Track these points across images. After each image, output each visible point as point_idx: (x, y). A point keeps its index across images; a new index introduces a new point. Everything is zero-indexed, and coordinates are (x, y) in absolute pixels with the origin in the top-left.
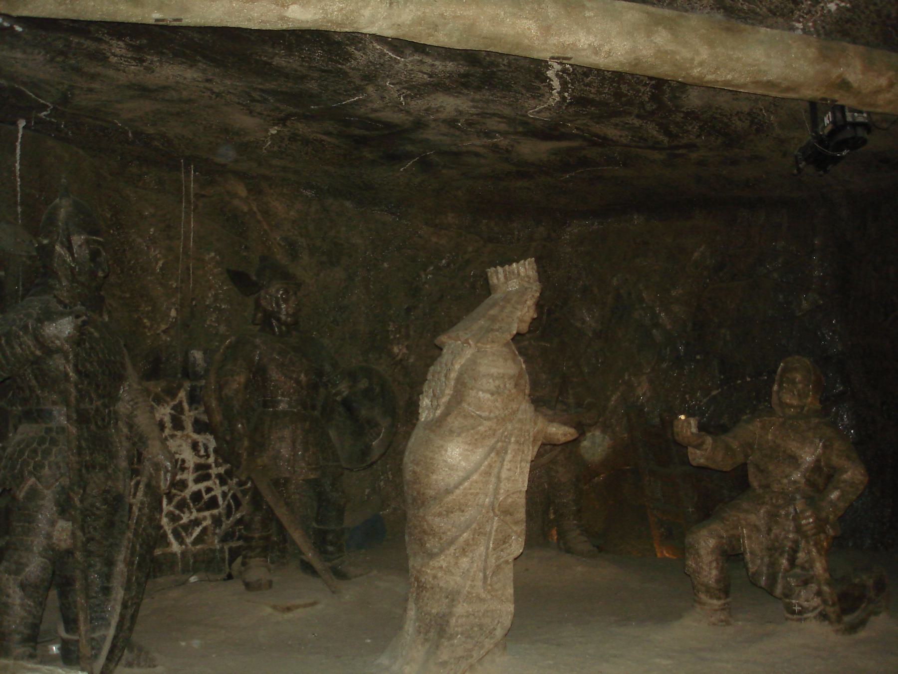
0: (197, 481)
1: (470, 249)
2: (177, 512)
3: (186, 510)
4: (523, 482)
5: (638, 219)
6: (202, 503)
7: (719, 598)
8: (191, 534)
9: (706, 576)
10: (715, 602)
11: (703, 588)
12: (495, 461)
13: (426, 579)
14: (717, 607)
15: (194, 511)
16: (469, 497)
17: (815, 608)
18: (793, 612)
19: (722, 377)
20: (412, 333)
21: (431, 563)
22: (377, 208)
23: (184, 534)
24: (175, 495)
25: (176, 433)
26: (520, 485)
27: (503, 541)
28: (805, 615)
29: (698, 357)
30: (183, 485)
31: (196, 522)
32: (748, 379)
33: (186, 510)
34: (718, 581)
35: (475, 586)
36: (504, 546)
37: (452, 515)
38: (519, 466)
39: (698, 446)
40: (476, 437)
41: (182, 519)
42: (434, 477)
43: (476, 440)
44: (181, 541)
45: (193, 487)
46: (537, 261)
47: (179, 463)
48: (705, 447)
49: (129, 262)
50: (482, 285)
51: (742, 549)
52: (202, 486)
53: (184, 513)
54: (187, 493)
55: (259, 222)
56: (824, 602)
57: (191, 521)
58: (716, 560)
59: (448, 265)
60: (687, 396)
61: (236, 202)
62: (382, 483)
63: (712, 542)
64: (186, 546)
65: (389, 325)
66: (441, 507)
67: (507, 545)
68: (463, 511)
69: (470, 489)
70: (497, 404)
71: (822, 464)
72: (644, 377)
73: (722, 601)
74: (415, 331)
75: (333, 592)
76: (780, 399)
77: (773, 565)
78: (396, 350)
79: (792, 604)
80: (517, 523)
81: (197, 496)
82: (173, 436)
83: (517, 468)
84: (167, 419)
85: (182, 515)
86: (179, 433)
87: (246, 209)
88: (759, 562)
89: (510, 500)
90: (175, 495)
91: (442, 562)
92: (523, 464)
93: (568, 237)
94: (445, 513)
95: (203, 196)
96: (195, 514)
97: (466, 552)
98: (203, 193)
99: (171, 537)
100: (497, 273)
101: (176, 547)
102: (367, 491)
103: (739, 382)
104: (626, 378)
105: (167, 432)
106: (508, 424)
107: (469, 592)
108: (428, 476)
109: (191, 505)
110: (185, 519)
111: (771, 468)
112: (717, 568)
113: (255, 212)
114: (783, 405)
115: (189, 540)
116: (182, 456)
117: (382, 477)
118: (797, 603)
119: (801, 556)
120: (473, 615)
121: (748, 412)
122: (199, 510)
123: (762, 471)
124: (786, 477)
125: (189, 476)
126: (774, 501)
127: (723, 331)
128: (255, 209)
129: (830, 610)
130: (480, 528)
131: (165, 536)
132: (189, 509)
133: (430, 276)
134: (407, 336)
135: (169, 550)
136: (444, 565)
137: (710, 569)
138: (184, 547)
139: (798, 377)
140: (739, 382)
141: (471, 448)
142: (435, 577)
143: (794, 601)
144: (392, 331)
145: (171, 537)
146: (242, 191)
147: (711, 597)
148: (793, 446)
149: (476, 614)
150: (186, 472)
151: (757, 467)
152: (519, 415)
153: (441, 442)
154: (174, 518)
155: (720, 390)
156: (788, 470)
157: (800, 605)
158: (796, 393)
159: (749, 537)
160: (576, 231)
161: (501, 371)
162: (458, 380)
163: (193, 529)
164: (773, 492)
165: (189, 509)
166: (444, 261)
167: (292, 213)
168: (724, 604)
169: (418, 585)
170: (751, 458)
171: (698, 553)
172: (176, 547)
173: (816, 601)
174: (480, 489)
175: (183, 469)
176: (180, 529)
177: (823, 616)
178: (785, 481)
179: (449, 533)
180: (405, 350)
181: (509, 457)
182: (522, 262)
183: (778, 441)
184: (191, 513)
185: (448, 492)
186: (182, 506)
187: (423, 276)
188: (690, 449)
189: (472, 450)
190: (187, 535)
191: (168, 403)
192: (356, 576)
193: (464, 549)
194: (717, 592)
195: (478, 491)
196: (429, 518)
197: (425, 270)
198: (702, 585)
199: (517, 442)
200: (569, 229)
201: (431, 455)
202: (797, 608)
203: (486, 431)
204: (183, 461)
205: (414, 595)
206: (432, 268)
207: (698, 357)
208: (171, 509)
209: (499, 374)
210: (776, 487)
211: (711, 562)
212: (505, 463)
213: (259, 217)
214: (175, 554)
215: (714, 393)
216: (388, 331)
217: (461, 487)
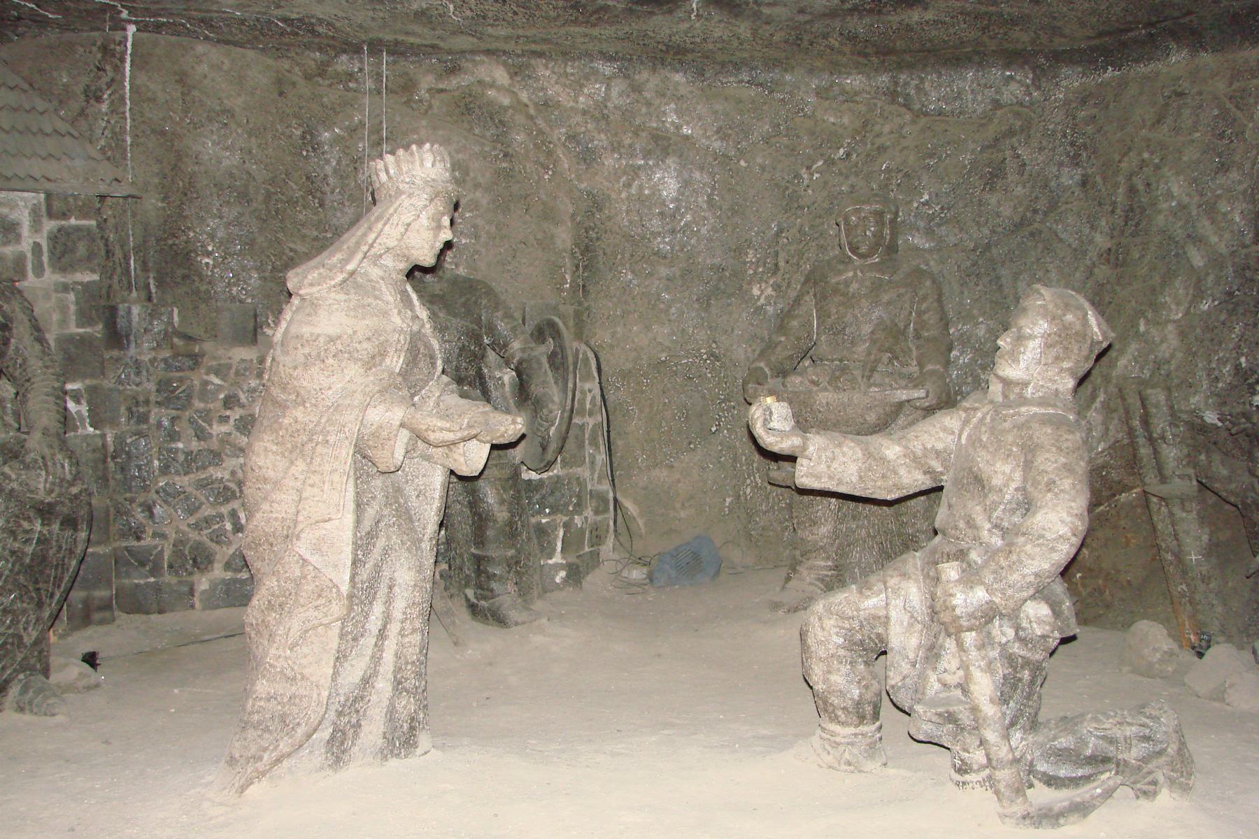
1: (887, 129)
14: (838, 739)
20: (782, 264)
22: (732, 79)
36: (319, 602)
50: (899, 185)
55: (531, 118)
59: (848, 155)
62: (749, 490)
65: (747, 254)
72: (1170, 327)
73: (851, 730)
75: (456, 644)
87: (506, 101)
93: (1061, 96)
95: (442, 91)
98: (441, 86)
102: (728, 500)
104: (1142, 328)
113: (526, 106)
117: (748, 481)
120: (276, 699)
133: (816, 176)
144: (752, 263)
149: (279, 698)
160: (1076, 84)
166: (842, 151)
167: (581, 99)
168: (856, 735)
180: (769, 291)
187: (805, 176)
192: (517, 624)
200: (1064, 83)
202: (958, 762)
206: (820, 163)
209: (312, 334)
213: (532, 111)
216: (745, 263)
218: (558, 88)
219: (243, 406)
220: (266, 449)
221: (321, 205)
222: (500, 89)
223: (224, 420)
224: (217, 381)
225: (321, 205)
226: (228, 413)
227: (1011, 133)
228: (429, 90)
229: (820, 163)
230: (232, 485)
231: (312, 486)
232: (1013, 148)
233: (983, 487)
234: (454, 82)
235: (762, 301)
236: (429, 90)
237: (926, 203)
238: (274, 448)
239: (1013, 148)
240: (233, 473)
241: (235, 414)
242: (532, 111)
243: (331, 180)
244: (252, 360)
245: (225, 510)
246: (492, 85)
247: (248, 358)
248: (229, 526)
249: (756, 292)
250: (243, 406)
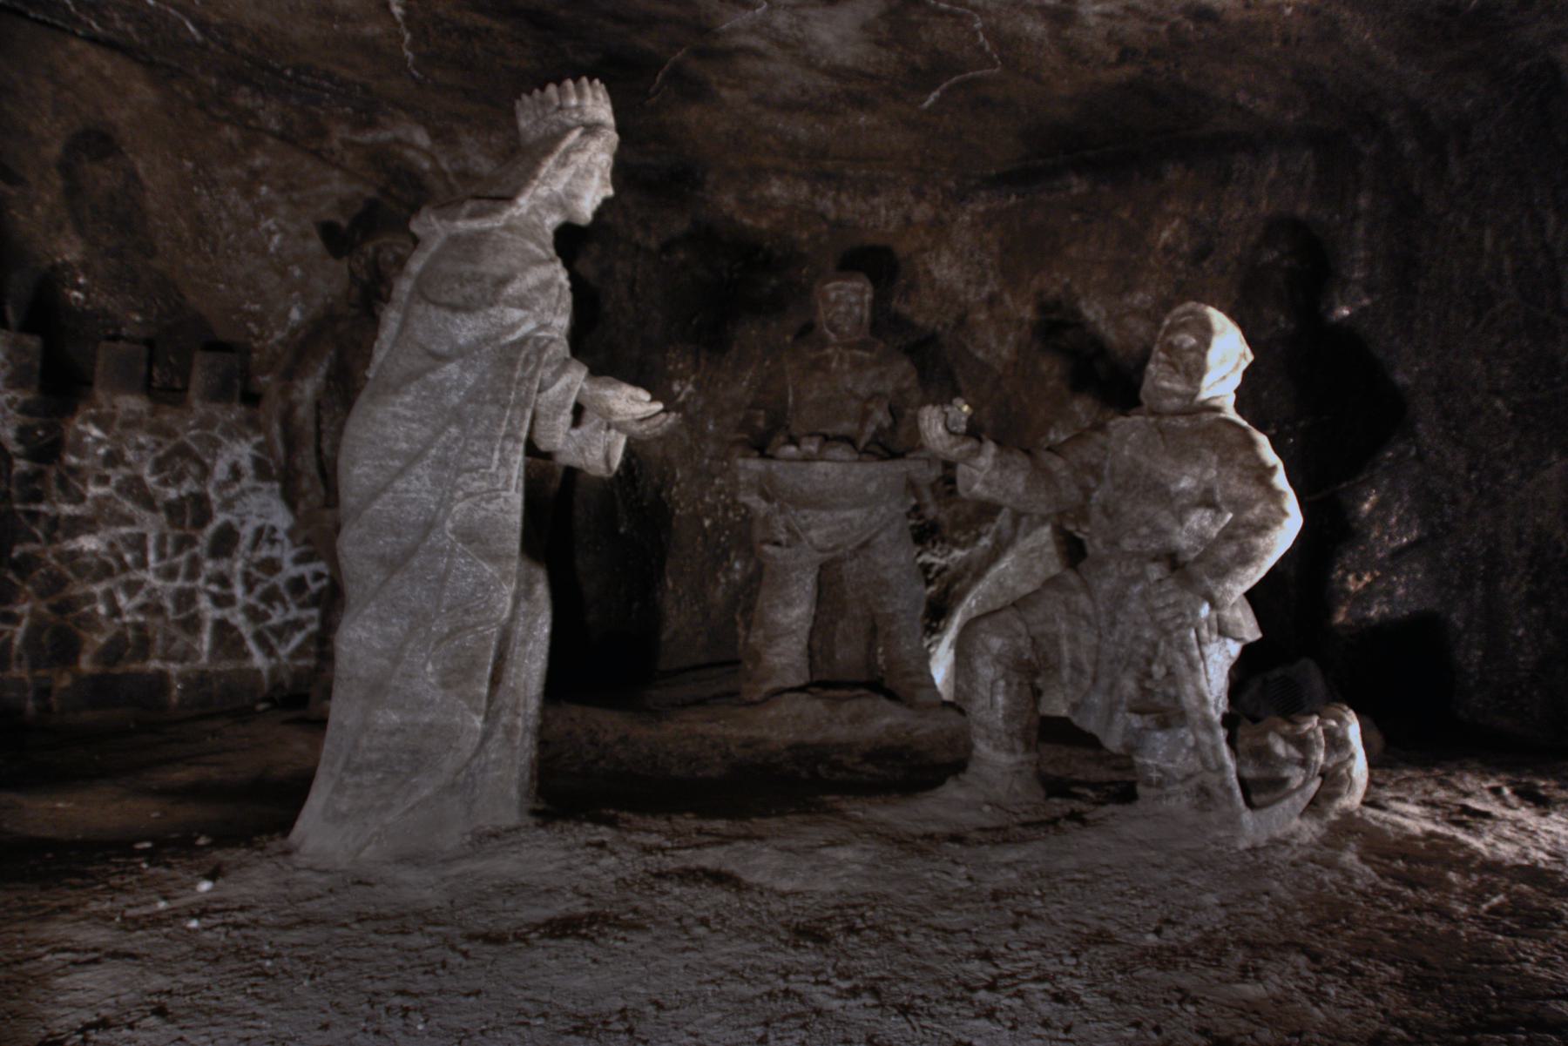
0: (299, 560)
2: (262, 607)
3: (277, 604)
5: (1078, 186)
6: (306, 596)
7: (1012, 751)
8: (287, 641)
9: (983, 708)
11: (982, 731)
15: (293, 607)
17: (1189, 776)
23: (274, 641)
24: (258, 581)
25: (260, 485)
28: (1169, 789)
30: (271, 566)
31: (297, 625)
33: (277, 604)
34: (1008, 718)
38: (498, 446)
40: (424, 393)
41: (268, 617)
42: (357, 471)
43: (424, 398)
44: (270, 652)
45: (290, 570)
47: (266, 531)
49: (227, 236)
52: (306, 570)
53: (273, 608)
54: (280, 580)
57: (287, 623)
58: (1004, 676)
61: (410, 154)
63: (996, 643)
64: (278, 658)
66: (360, 526)
71: (1218, 498)
80: (494, 558)
81: (298, 585)
82: (254, 490)
83: (492, 450)
84: (246, 463)
85: (270, 612)
86: (265, 486)
88: (1087, 683)
90: (258, 581)
91: (359, 629)
95: (353, 144)
96: (294, 613)
98: (358, 138)
99: (251, 645)
101: (259, 660)
105: (246, 482)
109: (288, 598)
110: (276, 618)
112: (1007, 693)
115: (284, 651)
116: (271, 522)
118: (1157, 766)
122: (302, 606)
124: (1147, 523)
125: (285, 553)
126: (1123, 570)
128: (444, 165)
131: (241, 640)
132: (283, 602)
135: (246, 665)
138: (273, 661)
142: (352, 661)
143: (1150, 762)
145: (251, 645)
146: (421, 138)
148: (1164, 467)
150: (278, 546)
154: (253, 614)
156: (1150, 510)
157: (1160, 770)
158: (1181, 368)
159: (1073, 638)
163: (292, 634)
164: (1124, 553)
165: (283, 602)
170: (1096, 494)
172: (259, 660)
175: (273, 542)
176: (268, 634)
180: (690, 388)
183: (1142, 458)
184: (287, 610)
185: (375, 495)
186: (270, 596)
190: (280, 642)
191: (247, 438)
194: (1005, 739)
198: (979, 724)
204: (274, 530)
208: (252, 600)
210: (1128, 544)
211: (994, 683)
214: (258, 671)
218: (481, 160)
219: (128, 465)
220: (395, 416)
221: (214, 251)
222: (418, 149)
223: (103, 480)
224: (96, 432)
225: (214, 251)
226: (108, 472)
228: (344, 143)
230: (112, 561)
231: (475, 454)
233: (1168, 493)
234: (368, 137)
235: (682, 398)
236: (344, 143)
238: (409, 414)
240: (111, 545)
241: (117, 475)
242: (452, 180)
243: (226, 226)
244: (142, 412)
245: (98, 589)
246: (412, 145)
247: (137, 408)
248: (102, 609)
249: (676, 388)
250: (128, 465)
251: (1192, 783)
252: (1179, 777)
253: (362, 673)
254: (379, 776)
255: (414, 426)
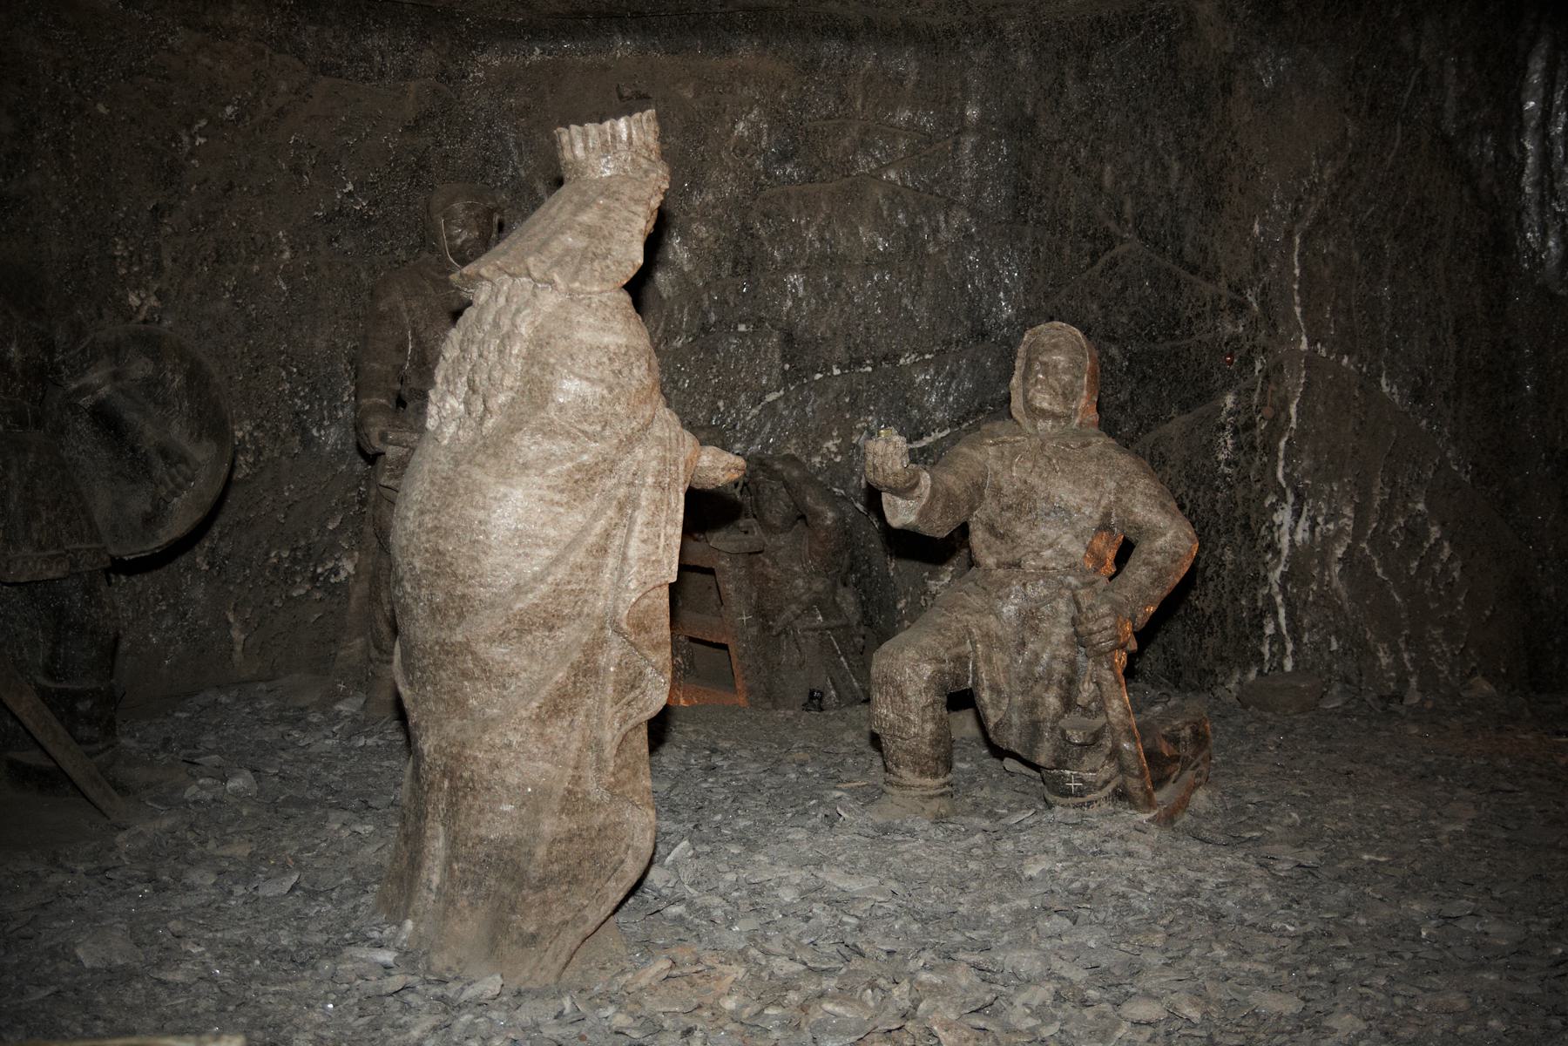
4: (670, 564)
7: (935, 775)
10: (929, 781)
12: (616, 524)
13: (472, 771)
14: (932, 792)
16: (565, 598)
17: (1107, 782)
18: (1067, 793)
19: (787, 366)
20: (167, 263)
21: (486, 738)
26: (664, 572)
27: (631, 684)
28: (1090, 797)
29: (742, 328)
32: (837, 372)
35: (580, 778)
36: (632, 695)
37: (529, 638)
39: (905, 491)
40: (577, 477)
46: (659, 118)
48: (917, 492)
51: (970, 682)
56: (1122, 769)
59: (239, 117)
60: (721, 404)
63: (927, 670)
65: (115, 244)
67: (638, 692)
68: (551, 629)
69: (569, 582)
70: (618, 408)
71: (1113, 521)
73: (941, 780)
74: (175, 260)
76: (1027, 402)
77: (1032, 706)
78: (134, 300)
79: (1065, 776)
80: (656, 647)
89: (646, 601)
92: (670, 530)
94: (515, 633)
97: (561, 710)
100: (585, 136)
103: (818, 376)
106: (637, 450)
107: (570, 792)
108: (474, 559)
111: (1020, 529)
114: (1035, 413)
119: (1086, 690)
121: (835, 434)
123: (1001, 537)
124: (1051, 546)
127: (792, 278)
129: (1134, 784)
130: (587, 662)
133: (200, 140)
134: (158, 267)
136: (515, 738)
137: (924, 721)
139: (1060, 359)
140: (818, 376)
141: (564, 498)
142: (495, 765)
144: (123, 258)
147: (922, 773)
151: (991, 528)
152: (656, 430)
153: (503, 489)
155: (782, 392)
161: (622, 341)
162: (531, 358)
166: (229, 110)
168: (944, 785)
169: (451, 787)
171: (901, 693)
173: (1108, 770)
174: (587, 581)
177: (1121, 795)
178: (1047, 553)
179: (523, 675)
180: (153, 301)
181: (641, 517)
182: (637, 116)
183: (1034, 480)
187: (186, 139)
188: (885, 497)
189: (567, 503)
193: (556, 706)
194: (931, 763)
195: (583, 585)
196: (481, 648)
197: (189, 127)
199: (658, 485)
201: (481, 515)
203: (597, 464)
205: (442, 806)
207: (742, 328)
209: (619, 347)
210: (1030, 563)
211: (924, 709)
212: (637, 528)
215: (770, 398)
217: (550, 579)
227: (430, 116)
229: (203, 123)
232: (435, 134)
237: (350, 194)
238: (557, 497)
239: (435, 134)
251: (1109, 788)
252: (1099, 784)
253: (513, 779)
254: (564, 888)
255: (562, 510)
